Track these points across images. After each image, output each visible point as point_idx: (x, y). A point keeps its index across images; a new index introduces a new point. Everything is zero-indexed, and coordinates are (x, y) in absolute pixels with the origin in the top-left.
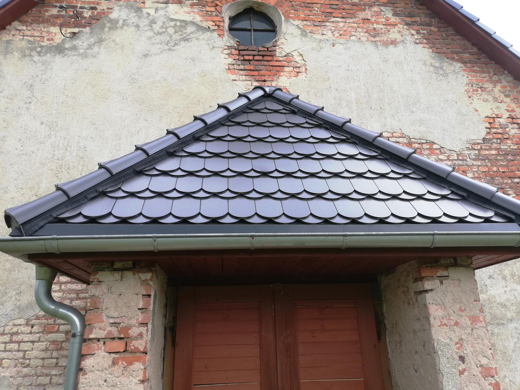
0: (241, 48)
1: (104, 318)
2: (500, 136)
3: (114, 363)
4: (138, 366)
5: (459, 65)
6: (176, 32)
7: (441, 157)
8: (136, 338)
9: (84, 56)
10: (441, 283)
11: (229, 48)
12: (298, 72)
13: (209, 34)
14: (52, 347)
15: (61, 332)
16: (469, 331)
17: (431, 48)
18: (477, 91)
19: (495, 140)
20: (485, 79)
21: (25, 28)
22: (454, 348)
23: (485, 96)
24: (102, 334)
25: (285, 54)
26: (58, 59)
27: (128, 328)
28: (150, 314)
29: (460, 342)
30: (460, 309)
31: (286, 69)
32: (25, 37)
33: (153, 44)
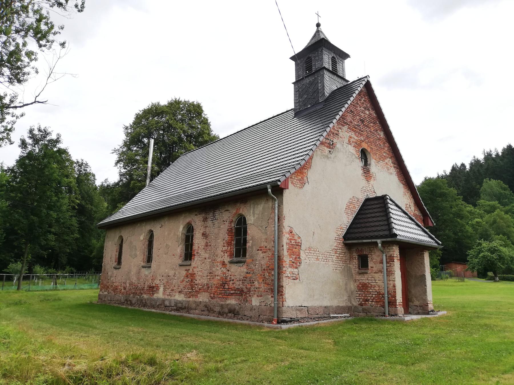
14: (337, 258)
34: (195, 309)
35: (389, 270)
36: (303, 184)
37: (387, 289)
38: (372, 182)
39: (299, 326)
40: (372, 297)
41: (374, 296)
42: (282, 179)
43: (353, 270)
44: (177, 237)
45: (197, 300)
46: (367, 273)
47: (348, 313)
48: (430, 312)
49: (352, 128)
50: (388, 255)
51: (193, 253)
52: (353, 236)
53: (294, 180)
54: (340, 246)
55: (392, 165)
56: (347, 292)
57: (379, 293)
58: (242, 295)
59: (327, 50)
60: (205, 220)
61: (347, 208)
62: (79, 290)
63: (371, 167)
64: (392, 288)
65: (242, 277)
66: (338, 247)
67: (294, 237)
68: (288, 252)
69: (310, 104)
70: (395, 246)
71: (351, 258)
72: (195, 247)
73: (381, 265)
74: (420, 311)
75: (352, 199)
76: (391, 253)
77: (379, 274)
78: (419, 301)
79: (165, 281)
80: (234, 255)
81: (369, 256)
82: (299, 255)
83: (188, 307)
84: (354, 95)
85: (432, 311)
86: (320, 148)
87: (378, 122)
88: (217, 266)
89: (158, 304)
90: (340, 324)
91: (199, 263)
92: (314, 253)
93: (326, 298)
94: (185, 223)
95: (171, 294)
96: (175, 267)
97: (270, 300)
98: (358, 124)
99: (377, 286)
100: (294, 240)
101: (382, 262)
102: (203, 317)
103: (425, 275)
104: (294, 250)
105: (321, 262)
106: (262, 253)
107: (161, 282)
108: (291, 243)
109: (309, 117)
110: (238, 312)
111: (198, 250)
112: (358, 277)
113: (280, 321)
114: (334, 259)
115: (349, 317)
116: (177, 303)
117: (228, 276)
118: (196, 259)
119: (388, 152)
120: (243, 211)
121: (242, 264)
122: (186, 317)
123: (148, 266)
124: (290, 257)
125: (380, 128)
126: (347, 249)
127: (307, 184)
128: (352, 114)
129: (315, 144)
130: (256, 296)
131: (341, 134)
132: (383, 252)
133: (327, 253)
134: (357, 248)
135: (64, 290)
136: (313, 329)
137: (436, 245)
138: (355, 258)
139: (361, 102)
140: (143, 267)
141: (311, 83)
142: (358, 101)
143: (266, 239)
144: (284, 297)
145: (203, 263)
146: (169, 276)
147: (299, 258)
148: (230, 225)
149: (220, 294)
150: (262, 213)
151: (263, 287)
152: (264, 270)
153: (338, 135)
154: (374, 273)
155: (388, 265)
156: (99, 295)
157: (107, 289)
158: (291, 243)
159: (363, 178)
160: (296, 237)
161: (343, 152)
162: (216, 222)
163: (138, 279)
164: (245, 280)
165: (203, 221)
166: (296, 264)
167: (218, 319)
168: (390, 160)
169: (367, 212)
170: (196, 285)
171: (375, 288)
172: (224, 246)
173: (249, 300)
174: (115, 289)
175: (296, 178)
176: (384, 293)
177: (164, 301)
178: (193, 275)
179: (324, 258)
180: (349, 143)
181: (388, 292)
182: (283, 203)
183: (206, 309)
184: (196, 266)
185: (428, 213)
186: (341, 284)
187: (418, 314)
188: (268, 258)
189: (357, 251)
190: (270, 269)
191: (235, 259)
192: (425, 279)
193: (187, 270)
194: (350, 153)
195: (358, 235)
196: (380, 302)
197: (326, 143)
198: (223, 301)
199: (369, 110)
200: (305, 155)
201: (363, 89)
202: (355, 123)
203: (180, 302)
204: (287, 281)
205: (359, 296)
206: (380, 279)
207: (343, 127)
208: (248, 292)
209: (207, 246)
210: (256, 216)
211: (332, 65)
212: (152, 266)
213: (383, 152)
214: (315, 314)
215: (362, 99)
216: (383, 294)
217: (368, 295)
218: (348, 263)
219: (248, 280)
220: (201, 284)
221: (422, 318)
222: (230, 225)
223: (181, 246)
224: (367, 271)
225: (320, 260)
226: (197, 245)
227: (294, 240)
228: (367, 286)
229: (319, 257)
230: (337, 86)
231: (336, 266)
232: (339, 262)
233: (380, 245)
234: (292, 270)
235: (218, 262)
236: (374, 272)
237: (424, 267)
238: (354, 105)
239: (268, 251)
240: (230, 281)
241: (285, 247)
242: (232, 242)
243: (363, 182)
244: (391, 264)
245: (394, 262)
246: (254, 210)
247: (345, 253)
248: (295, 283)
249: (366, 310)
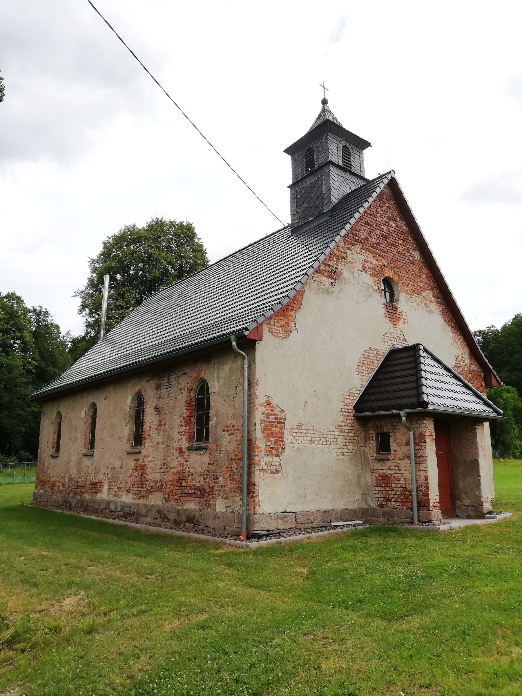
14: (343, 438)
34: (146, 516)
35: (418, 455)
36: (287, 332)
37: (417, 483)
38: (401, 325)
39: (277, 543)
40: (396, 494)
41: (398, 493)
42: (252, 326)
43: (369, 456)
44: (124, 414)
45: (148, 502)
46: (388, 460)
47: (361, 519)
48: (486, 514)
49: (368, 247)
50: (417, 434)
51: (143, 436)
52: (368, 405)
53: (274, 327)
54: (348, 421)
55: (433, 299)
56: (360, 487)
57: (405, 490)
58: (203, 497)
59: (334, 136)
60: (158, 388)
61: (361, 364)
62: (28, 483)
63: (400, 303)
64: (423, 481)
65: (203, 470)
66: (346, 422)
67: (273, 411)
68: (263, 433)
69: (311, 216)
70: (427, 419)
71: (366, 438)
72: (146, 427)
73: (408, 447)
74: (471, 513)
75: (369, 351)
76: (422, 429)
77: (405, 461)
78: (469, 499)
79: (111, 474)
80: (194, 438)
81: (391, 434)
82: (282, 437)
83: (137, 513)
84: (370, 200)
85: (490, 513)
86: (316, 279)
87: (410, 238)
88: (173, 455)
89: (101, 507)
90: (339, 539)
91: (150, 450)
92: (306, 433)
93: (325, 497)
94: (134, 393)
95: (117, 493)
96: (121, 455)
97: (237, 503)
98: (378, 241)
99: (402, 479)
100: (274, 415)
101: (408, 444)
102: (152, 528)
103: (477, 461)
104: (273, 429)
105: (318, 446)
106: (229, 435)
107: (105, 476)
108: (268, 420)
109: (307, 235)
110: (198, 521)
111: (150, 432)
112: (377, 466)
113: (250, 535)
114: (339, 440)
115: (362, 524)
116: (124, 506)
117: (186, 468)
118: (147, 444)
119: (426, 281)
120: (205, 374)
121: (204, 451)
122: (132, 527)
123: (90, 453)
124: (267, 441)
125: (414, 246)
126: (359, 424)
127: (294, 332)
128: (369, 227)
129: (306, 274)
130: (220, 498)
131: (350, 257)
132: (409, 429)
134: (375, 423)
135: (9, 484)
136: (292, 548)
137: (495, 415)
138: (373, 437)
139: (383, 209)
140: (85, 455)
141: (313, 186)
142: (379, 207)
143: (234, 415)
144: (256, 500)
145: (156, 449)
146: (115, 468)
147: (282, 441)
148: (189, 395)
149: (177, 494)
150: (229, 377)
151: (230, 485)
152: (231, 460)
153: (345, 259)
154: (399, 459)
155: (417, 447)
156: (34, 494)
157: (43, 486)
158: (268, 420)
159: (387, 320)
160: (276, 411)
161: (353, 284)
162: (172, 391)
163: (79, 471)
164: (207, 475)
165: (156, 389)
166: (277, 450)
167: (169, 531)
168: (431, 292)
169: (390, 369)
170: (147, 481)
171: (400, 482)
172: (181, 426)
173: (212, 504)
174: (53, 486)
175: (276, 324)
176: (411, 489)
177: (108, 503)
178: (143, 467)
179: (322, 439)
180: (364, 269)
181: (417, 488)
182: (255, 361)
183: (159, 516)
184: (147, 454)
185: (491, 367)
186: (350, 477)
187: (469, 517)
188: (236, 442)
189: (374, 427)
190: (238, 459)
191: (195, 444)
192: (478, 466)
193: (137, 460)
194: (365, 285)
195: (374, 405)
196: (406, 502)
197: (325, 270)
198: (179, 505)
199: (395, 221)
200: (291, 289)
201: (386, 191)
202: (374, 240)
203: (128, 506)
204: (262, 476)
205: (378, 494)
206: (406, 468)
207: (353, 247)
208: (211, 493)
209: (160, 425)
210: (221, 381)
211: (343, 158)
212: (95, 454)
213: (419, 280)
214: (307, 523)
215: (384, 205)
216: (411, 491)
217: (390, 492)
218: (362, 445)
219: (211, 474)
220: (153, 480)
221: (467, 527)
222: (189, 395)
223: (129, 426)
224: (388, 457)
225: (317, 443)
226: (148, 424)
227: (274, 415)
228: (389, 479)
229: (314, 439)
230: (350, 188)
231: (343, 450)
232: (348, 444)
233: (404, 418)
234: (271, 460)
235: (173, 449)
236: (398, 457)
237: (477, 448)
238: (371, 215)
239: (237, 432)
240: (189, 475)
241: (259, 427)
242: (192, 419)
243: (386, 326)
244: (421, 445)
245: (425, 442)
246: (218, 373)
247: (357, 431)
248: (274, 478)
249: (387, 513)
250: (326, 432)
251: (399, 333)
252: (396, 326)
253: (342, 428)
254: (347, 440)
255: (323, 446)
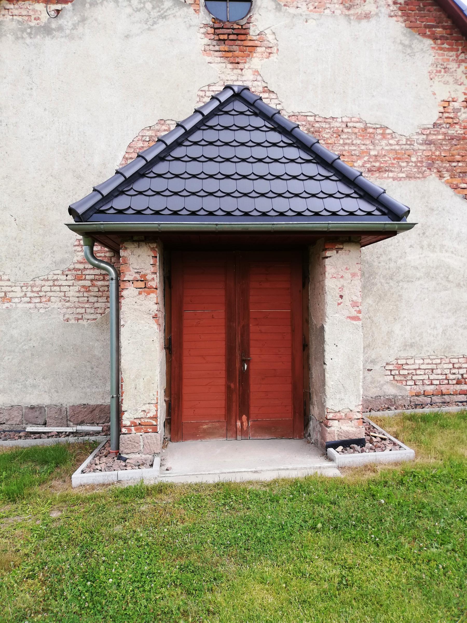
0: (216, 26)
1: (131, 269)
2: (450, 121)
3: (140, 293)
4: (153, 295)
5: (429, 42)
6: (153, 8)
7: (391, 142)
8: (151, 281)
9: (71, 37)
10: (337, 252)
11: (206, 25)
12: (270, 53)
13: (185, 9)
14: (83, 290)
15: (88, 280)
16: (349, 281)
17: (405, 21)
18: (440, 72)
19: (444, 125)
20: (451, 58)
21: (11, 6)
22: (338, 291)
23: (447, 78)
24: (131, 278)
25: (258, 32)
26: (48, 41)
27: (145, 275)
28: (158, 267)
29: (342, 288)
30: (347, 269)
31: (259, 49)
32: (15, 17)
33: (134, 23)
48: (335, 445)
75: (157, 127)
86: (16, 12)
93: (34, 386)
105: (19, 305)
133: (43, 283)
159: (216, 58)
179: (29, 294)
229: (9, 295)
250: (38, 282)
251: (252, 78)
252: (241, 66)
253: (79, 272)
254: (92, 294)
255: (31, 305)
